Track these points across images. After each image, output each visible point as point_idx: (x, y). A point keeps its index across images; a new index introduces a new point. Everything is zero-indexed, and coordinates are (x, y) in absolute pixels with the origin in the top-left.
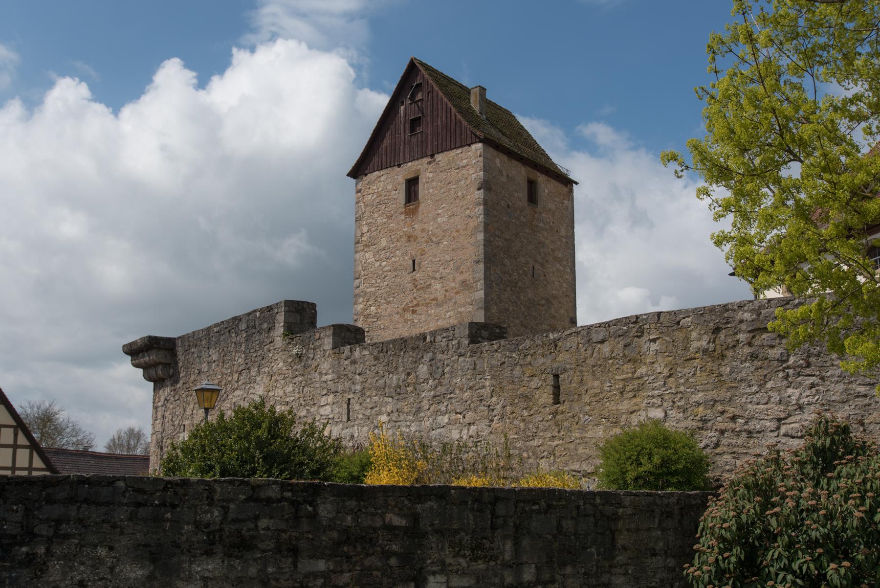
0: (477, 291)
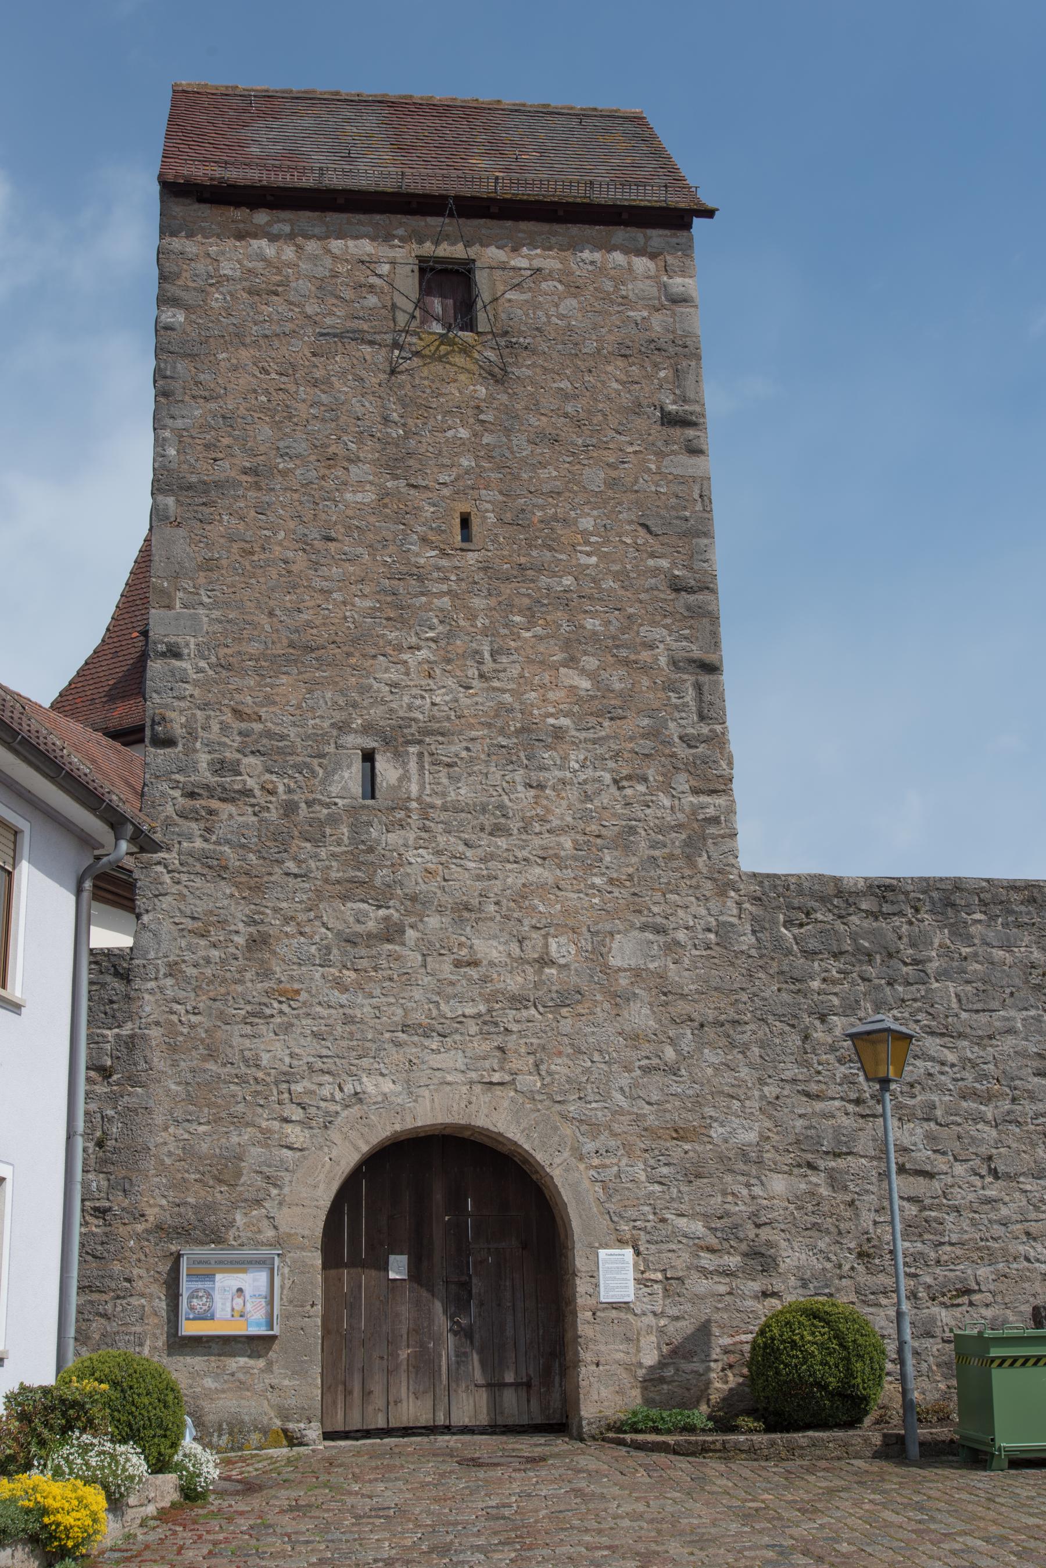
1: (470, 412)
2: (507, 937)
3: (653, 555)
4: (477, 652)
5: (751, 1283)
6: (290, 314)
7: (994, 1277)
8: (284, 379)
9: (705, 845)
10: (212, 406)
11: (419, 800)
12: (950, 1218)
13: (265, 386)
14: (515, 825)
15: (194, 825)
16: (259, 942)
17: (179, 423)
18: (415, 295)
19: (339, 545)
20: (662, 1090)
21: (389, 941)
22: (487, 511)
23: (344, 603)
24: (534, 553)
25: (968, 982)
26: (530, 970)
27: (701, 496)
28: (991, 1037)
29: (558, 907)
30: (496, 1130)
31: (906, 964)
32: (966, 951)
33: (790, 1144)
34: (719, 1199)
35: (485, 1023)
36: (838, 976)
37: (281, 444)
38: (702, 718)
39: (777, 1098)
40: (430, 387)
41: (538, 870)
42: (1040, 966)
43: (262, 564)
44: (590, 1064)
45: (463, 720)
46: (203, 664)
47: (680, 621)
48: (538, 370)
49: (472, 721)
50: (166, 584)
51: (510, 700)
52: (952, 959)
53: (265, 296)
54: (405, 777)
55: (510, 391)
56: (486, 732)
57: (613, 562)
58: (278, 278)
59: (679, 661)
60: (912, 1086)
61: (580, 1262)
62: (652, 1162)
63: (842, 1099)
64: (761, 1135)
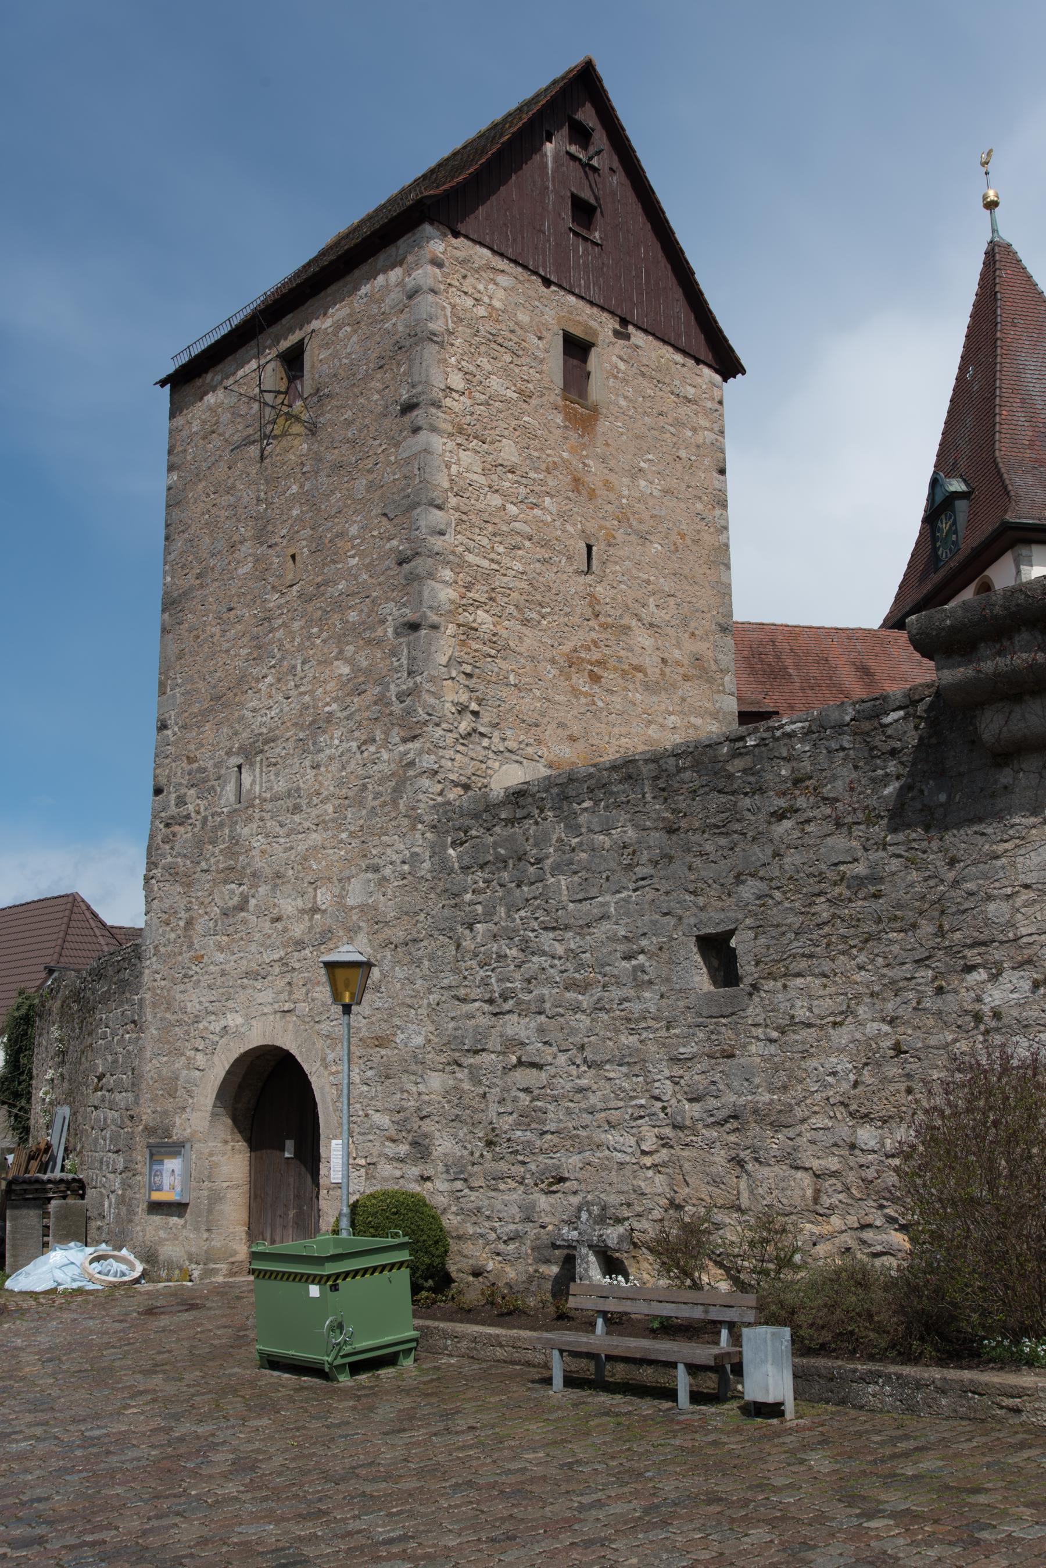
0: (724, 692)
2: (296, 894)
7: (581, 1165)
12: (551, 1107)
14: (304, 802)
25: (575, 873)
26: (306, 917)
28: (588, 925)
29: (323, 863)
33: (444, 1045)
39: (438, 1004)
41: (314, 836)
42: (631, 845)
60: (529, 981)
64: (426, 1039)
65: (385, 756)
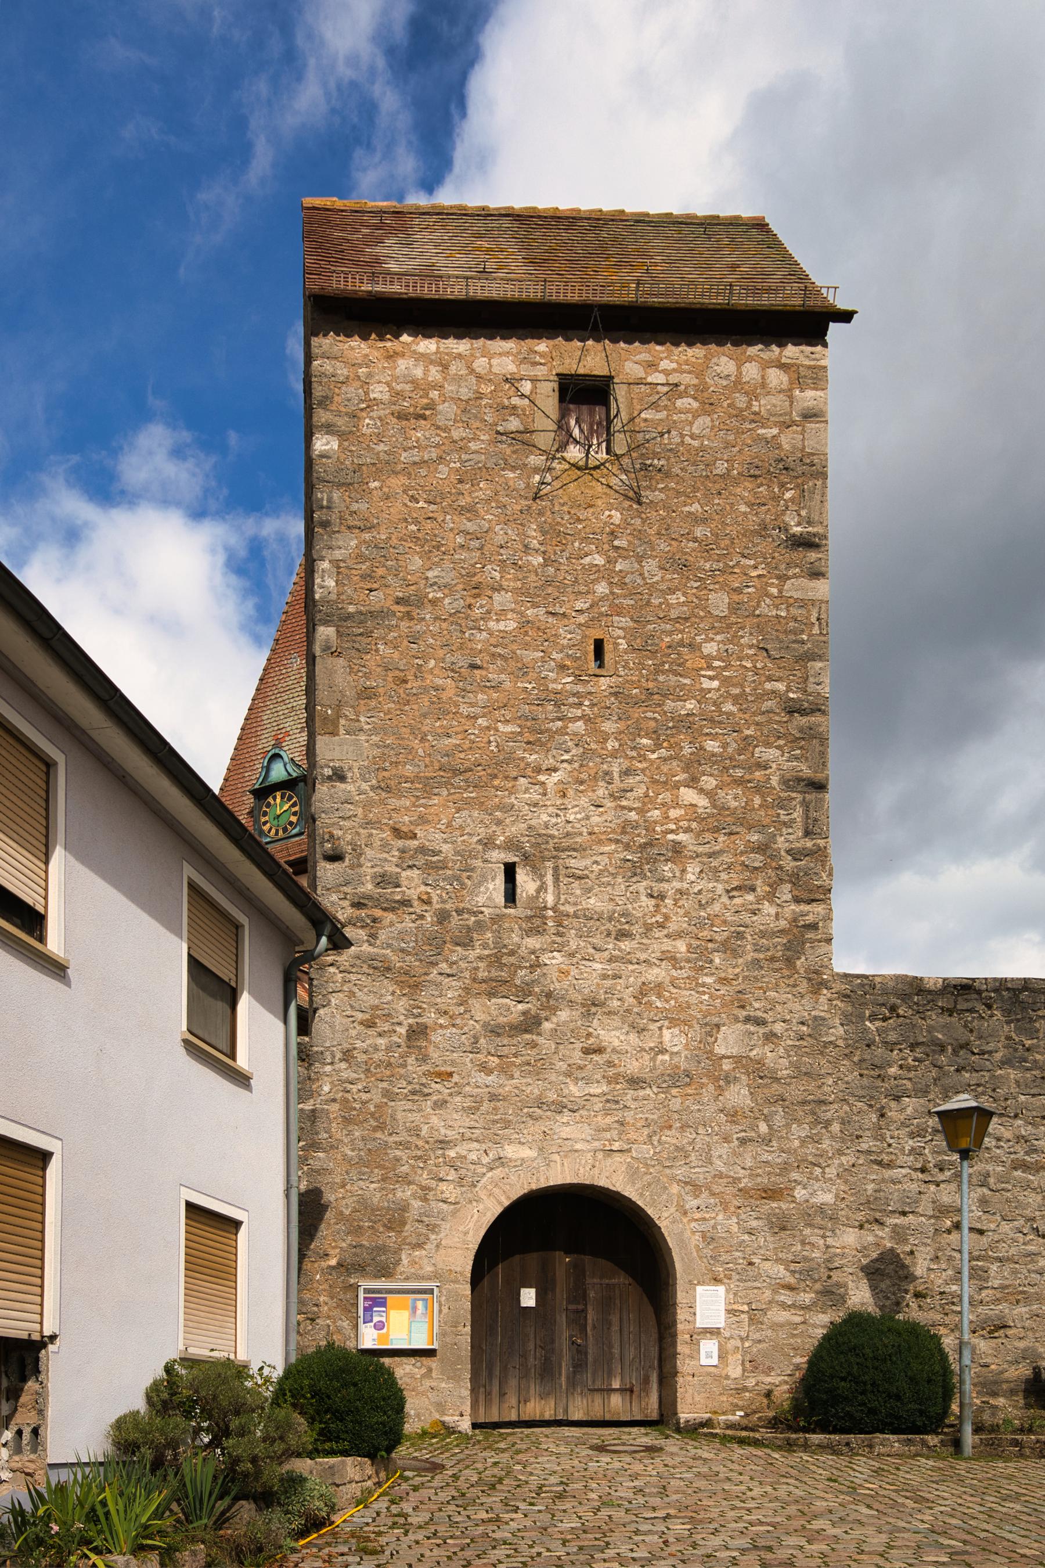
1: (605, 538)
3: (770, 679)
4: (607, 773)
5: (821, 1316)
6: (438, 439)
7: (1028, 1316)
8: (433, 507)
9: (803, 949)
10: (367, 536)
11: (554, 909)
12: (994, 1267)
13: (415, 515)
14: (636, 929)
15: (360, 931)
16: (418, 1033)
17: (338, 554)
18: (554, 414)
19: (484, 673)
20: (755, 1158)
21: (526, 1031)
22: (619, 637)
23: (488, 728)
24: (661, 678)
26: (647, 1057)
27: (818, 619)
30: (614, 1189)
31: (974, 1053)
32: (1028, 1043)
34: (799, 1247)
35: (608, 1101)
36: (913, 1063)
37: (430, 574)
38: (807, 833)
39: (853, 1165)
40: (569, 513)
43: (414, 691)
44: (695, 1135)
45: (593, 837)
46: (365, 786)
47: (791, 742)
48: (671, 493)
49: (603, 837)
50: (329, 712)
51: (636, 817)
52: (1016, 1050)
53: (413, 421)
54: (542, 888)
55: (643, 516)
56: (613, 847)
57: (733, 686)
58: (425, 401)
59: (789, 780)
61: (681, 1297)
62: (743, 1216)
63: (910, 1167)
64: (837, 1196)
65: (769, 909)
